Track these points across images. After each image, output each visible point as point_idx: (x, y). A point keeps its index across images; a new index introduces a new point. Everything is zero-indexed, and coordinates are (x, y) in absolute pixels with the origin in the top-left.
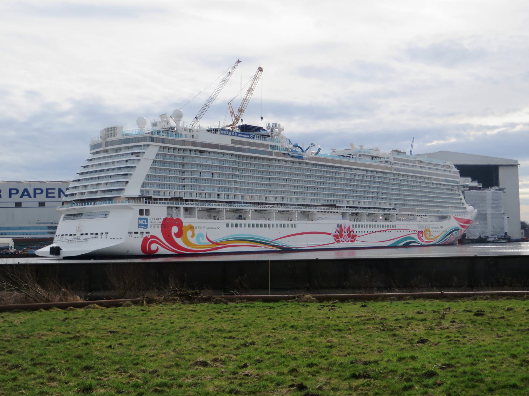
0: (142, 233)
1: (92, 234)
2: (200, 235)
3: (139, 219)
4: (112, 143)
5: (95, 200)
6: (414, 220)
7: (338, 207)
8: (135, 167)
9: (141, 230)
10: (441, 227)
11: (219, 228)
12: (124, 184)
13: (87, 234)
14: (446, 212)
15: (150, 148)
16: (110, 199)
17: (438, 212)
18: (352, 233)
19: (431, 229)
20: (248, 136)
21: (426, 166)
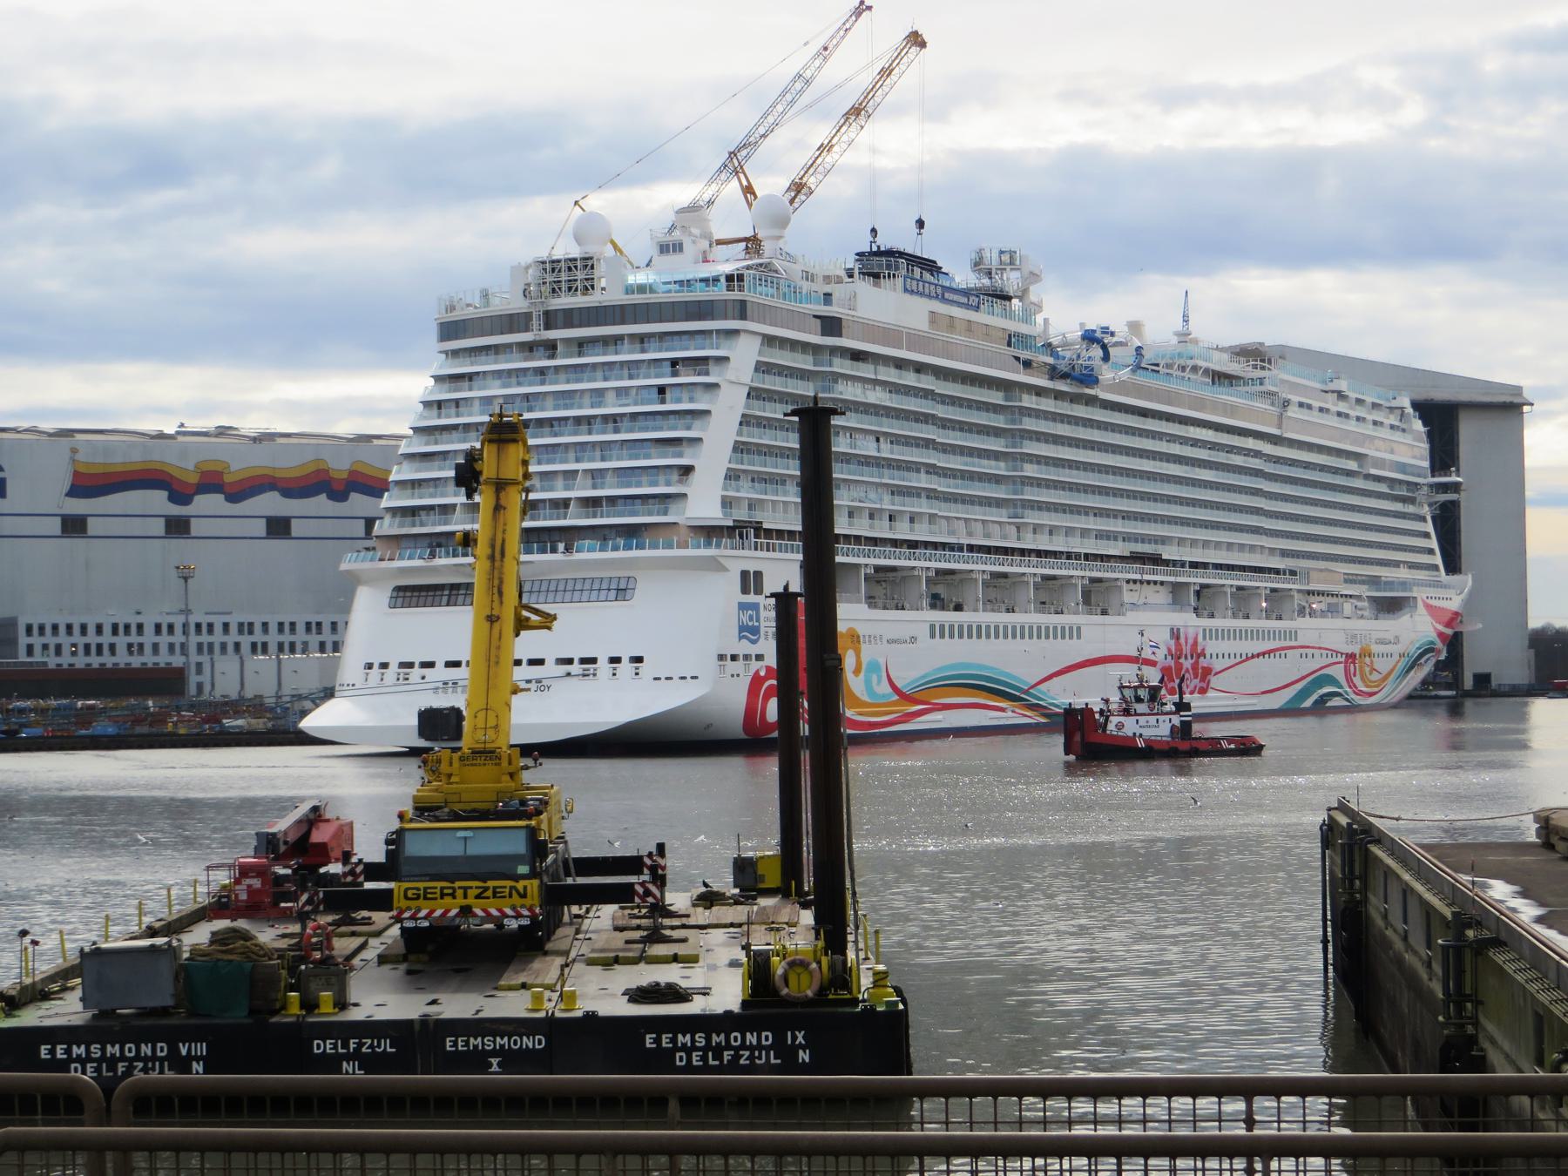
0: (747, 657)
1: (570, 661)
2: (874, 667)
3: (743, 607)
4: (570, 318)
5: (569, 536)
6: (1333, 611)
7: (1166, 563)
8: (708, 412)
9: (744, 648)
10: (1397, 641)
11: (913, 639)
12: (675, 477)
13: (540, 662)
14: (1404, 585)
15: (743, 338)
16: (632, 533)
17: (1374, 581)
18: (1203, 662)
19: (1375, 648)
20: (964, 300)
21: (1353, 413)
